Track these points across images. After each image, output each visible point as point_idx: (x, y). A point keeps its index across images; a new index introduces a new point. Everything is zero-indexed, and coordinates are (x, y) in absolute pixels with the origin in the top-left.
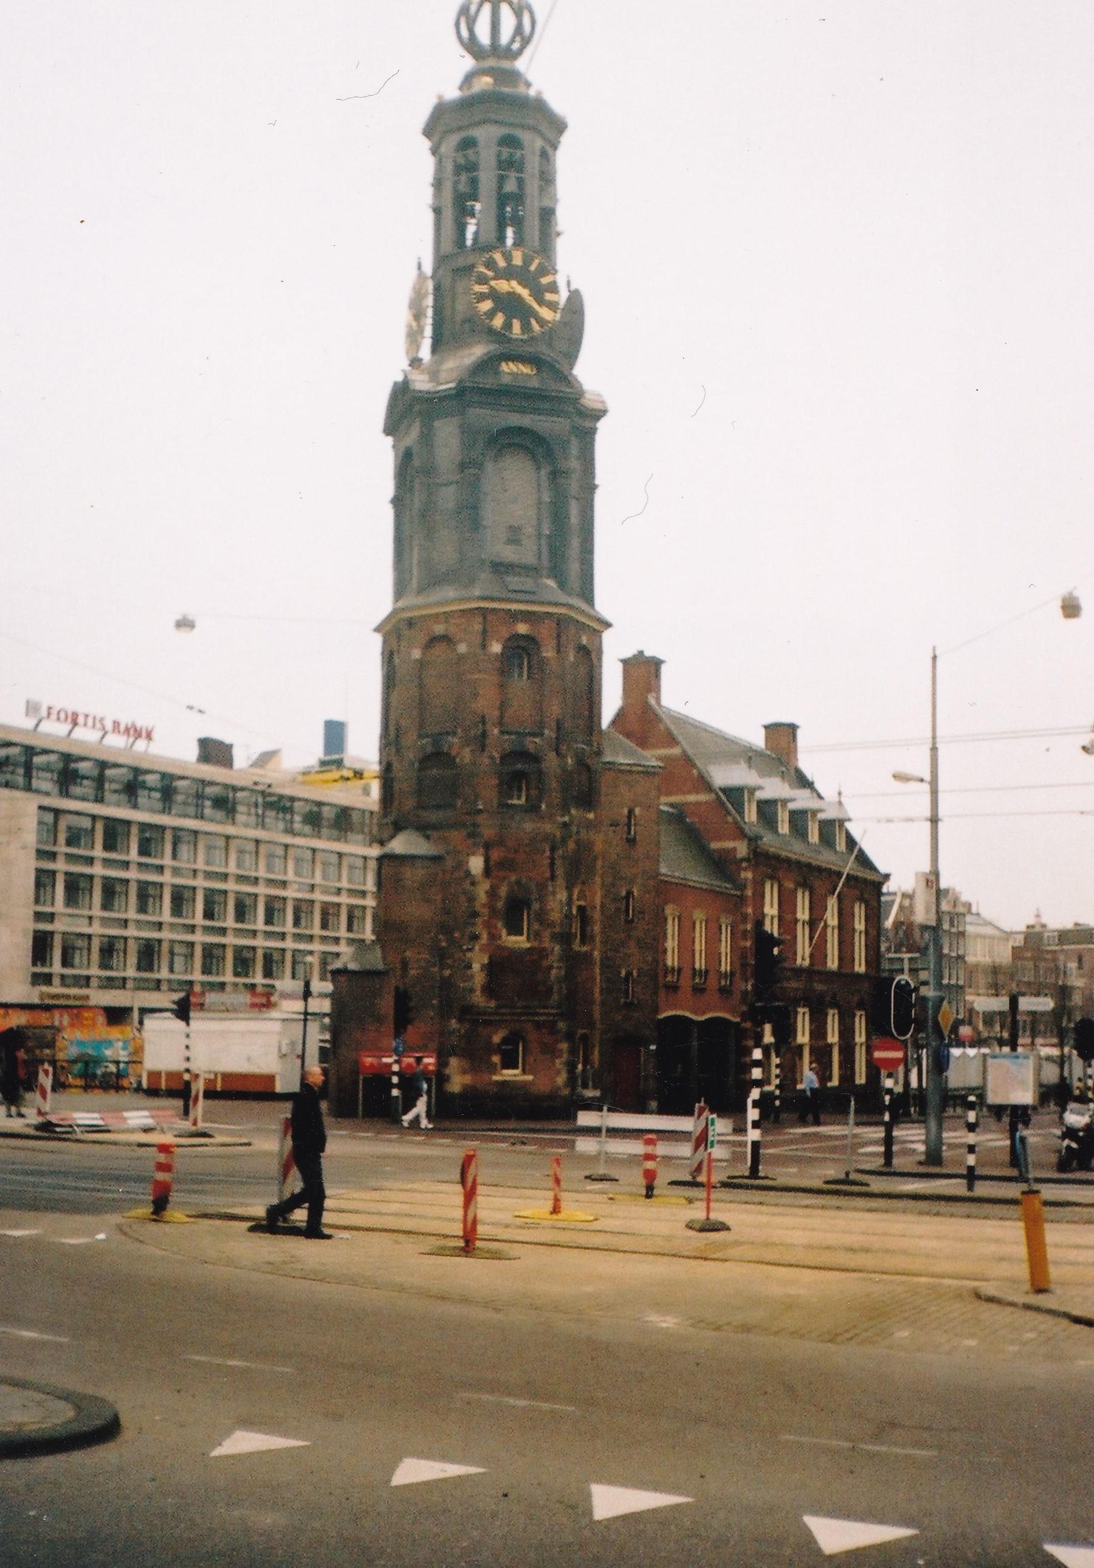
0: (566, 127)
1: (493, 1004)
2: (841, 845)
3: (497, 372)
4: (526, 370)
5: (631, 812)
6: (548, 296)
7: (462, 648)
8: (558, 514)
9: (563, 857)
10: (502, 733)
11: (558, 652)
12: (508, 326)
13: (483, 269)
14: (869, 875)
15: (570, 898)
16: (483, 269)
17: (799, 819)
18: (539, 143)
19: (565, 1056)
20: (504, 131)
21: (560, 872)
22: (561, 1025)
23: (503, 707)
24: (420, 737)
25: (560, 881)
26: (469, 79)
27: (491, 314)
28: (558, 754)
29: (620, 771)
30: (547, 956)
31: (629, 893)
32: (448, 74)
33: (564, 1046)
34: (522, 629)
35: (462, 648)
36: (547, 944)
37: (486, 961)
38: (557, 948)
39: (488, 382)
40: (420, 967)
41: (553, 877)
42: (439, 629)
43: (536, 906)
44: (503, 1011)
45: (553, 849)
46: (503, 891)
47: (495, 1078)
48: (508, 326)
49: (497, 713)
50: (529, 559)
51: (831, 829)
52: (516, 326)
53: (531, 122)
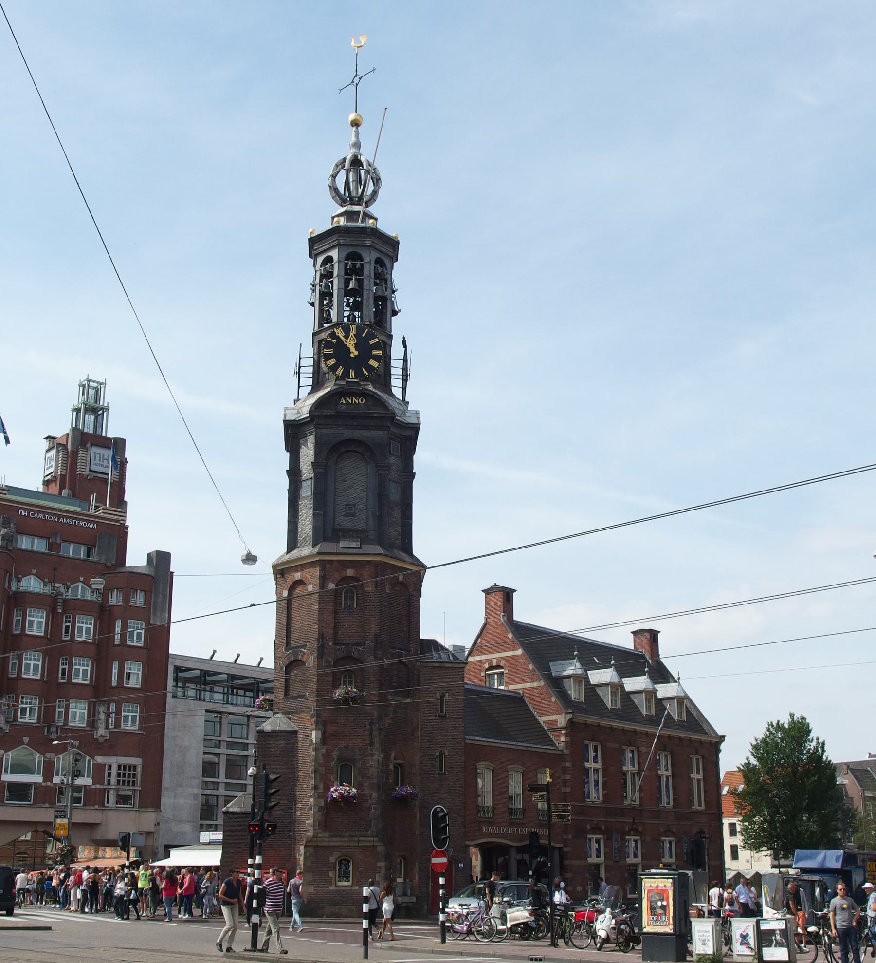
0: (398, 243)
1: (327, 835)
5: (442, 696)
8: (381, 496)
9: (380, 729)
10: (335, 644)
11: (376, 587)
15: (386, 759)
18: (374, 255)
19: (383, 871)
20: (351, 250)
21: (377, 741)
22: (379, 849)
23: (336, 628)
24: (287, 650)
25: (377, 745)
29: (434, 667)
30: (367, 801)
31: (441, 755)
33: (382, 864)
34: (350, 572)
36: (367, 791)
37: (322, 804)
38: (375, 795)
40: (282, 810)
41: (372, 744)
42: (298, 576)
43: (359, 764)
44: (334, 839)
45: (371, 724)
46: (335, 754)
47: (332, 888)
49: (331, 631)
50: (361, 525)
53: (368, 243)
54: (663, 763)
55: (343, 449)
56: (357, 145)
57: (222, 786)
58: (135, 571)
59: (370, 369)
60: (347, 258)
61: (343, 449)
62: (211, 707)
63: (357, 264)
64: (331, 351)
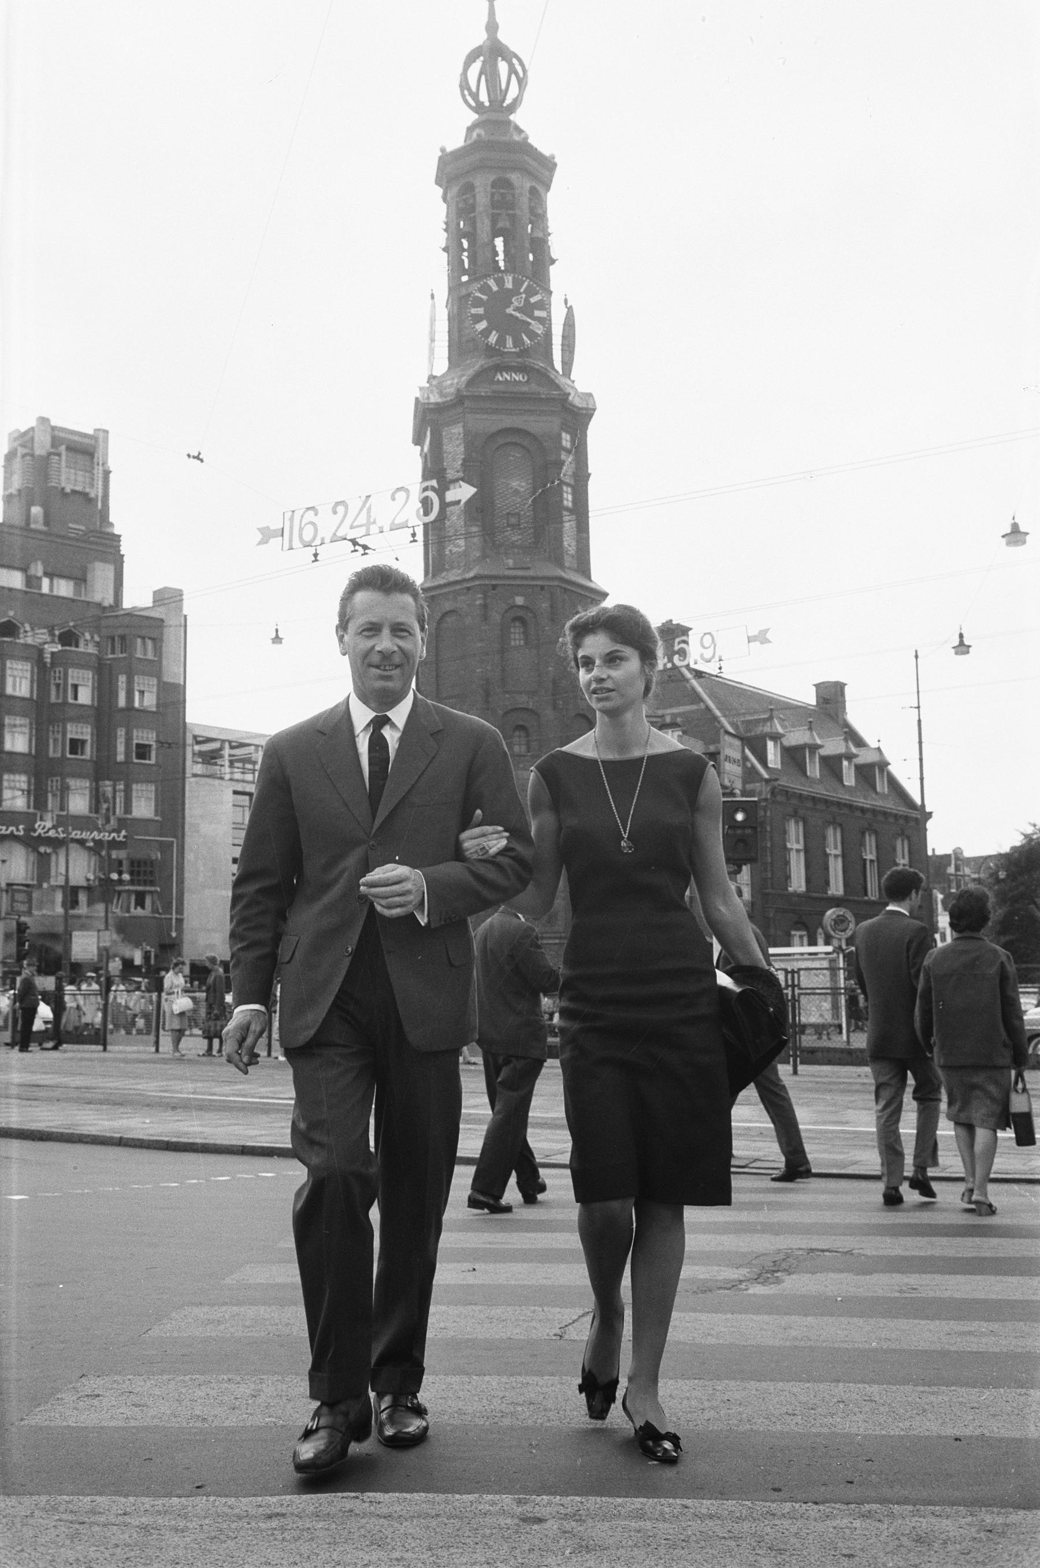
2: (882, 786)
3: (492, 382)
4: (518, 377)
6: (537, 313)
7: (468, 620)
12: (501, 341)
13: (478, 294)
14: (914, 814)
16: (478, 294)
17: (832, 765)
26: (470, 130)
27: (486, 333)
28: (554, 708)
32: (454, 126)
34: (519, 600)
35: (468, 620)
39: (483, 390)
48: (501, 341)
51: (873, 772)
52: (509, 342)
55: (501, 441)
56: (492, 27)
59: (532, 335)
60: (494, 185)
61: (501, 441)
62: (239, 787)
63: (496, 192)
64: (481, 311)
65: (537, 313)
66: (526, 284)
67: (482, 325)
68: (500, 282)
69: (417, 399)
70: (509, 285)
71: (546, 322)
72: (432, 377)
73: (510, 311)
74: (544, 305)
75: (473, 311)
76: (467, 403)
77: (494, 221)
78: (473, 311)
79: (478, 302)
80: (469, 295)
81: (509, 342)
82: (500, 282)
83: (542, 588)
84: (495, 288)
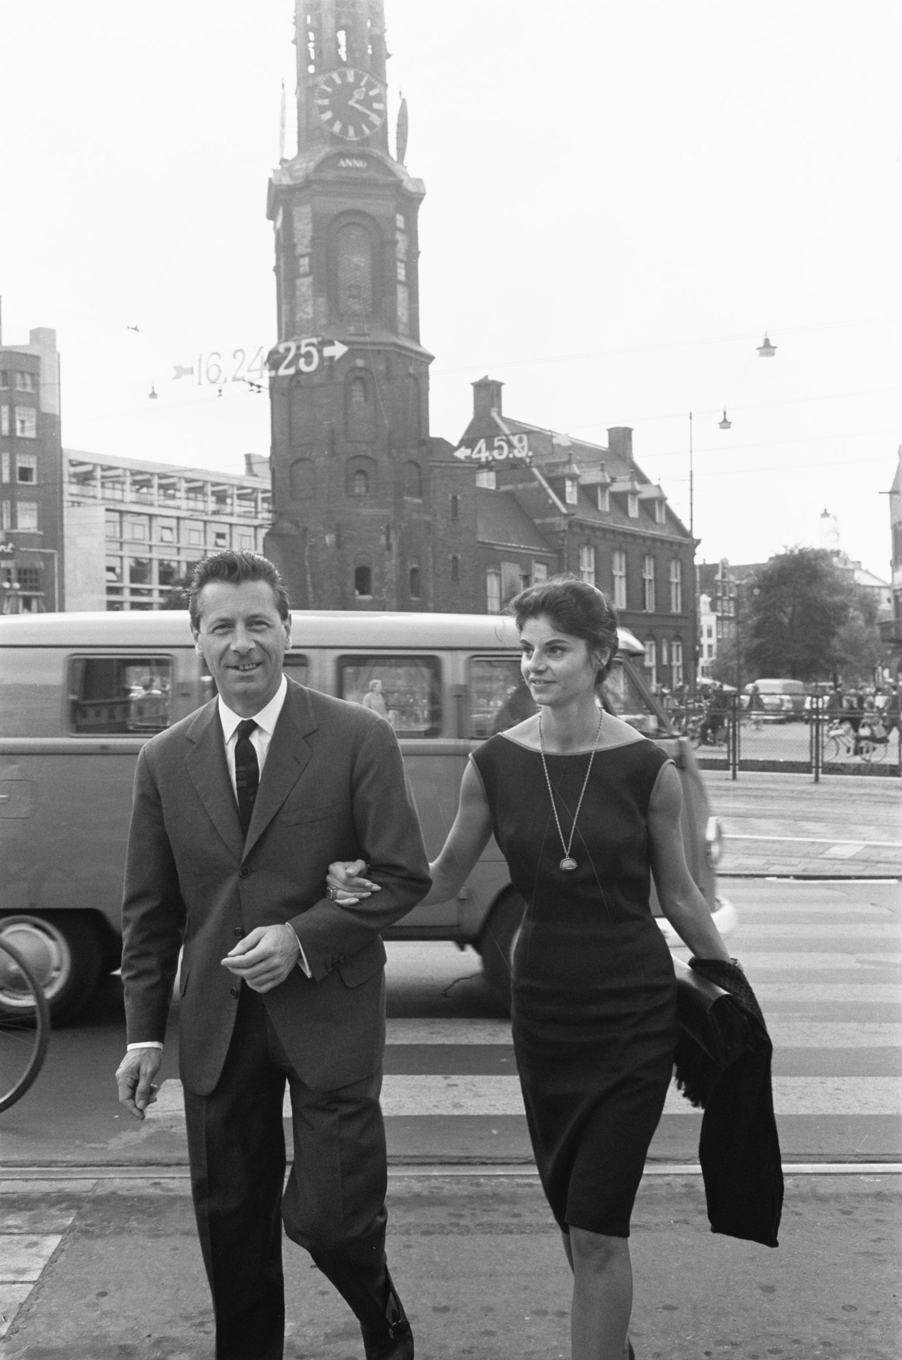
2: (660, 517)
4: (359, 164)
6: (376, 106)
12: (344, 130)
13: (325, 87)
14: (686, 541)
16: (325, 87)
27: (331, 122)
48: (344, 130)
51: (652, 505)
52: (351, 131)
54: (673, 570)
55: (344, 221)
57: (127, 592)
58: (14, 350)
59: (371, 126)
64: (326, 102)
65: (376, 106)
66: (366, 78)
67: (328, 115)
68: (343, 76)
69: (270, 180)
70: (351, 78)
71: (383, 114)
72: (283, 161)
73: (352, 103)
74: (381, 98)
75: (320, 102)
76: (315, 187)
77: (338, 17)
78: (320, 102)
79: (323, 95)
80: (316, 86)
81: (351, 131)
82: (343, 76)
83: (379, 352)
84: (339, 81)
